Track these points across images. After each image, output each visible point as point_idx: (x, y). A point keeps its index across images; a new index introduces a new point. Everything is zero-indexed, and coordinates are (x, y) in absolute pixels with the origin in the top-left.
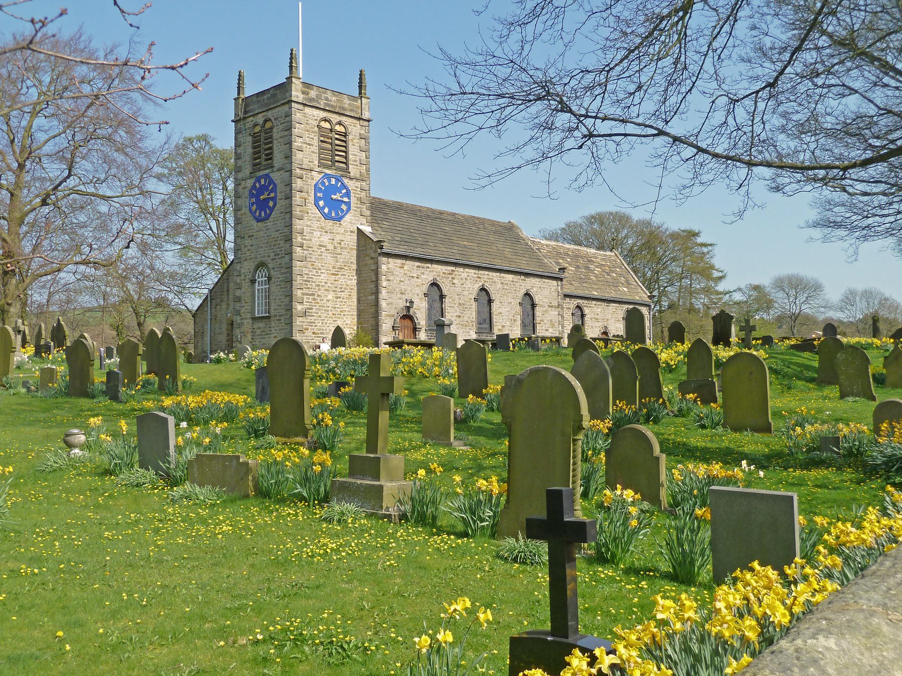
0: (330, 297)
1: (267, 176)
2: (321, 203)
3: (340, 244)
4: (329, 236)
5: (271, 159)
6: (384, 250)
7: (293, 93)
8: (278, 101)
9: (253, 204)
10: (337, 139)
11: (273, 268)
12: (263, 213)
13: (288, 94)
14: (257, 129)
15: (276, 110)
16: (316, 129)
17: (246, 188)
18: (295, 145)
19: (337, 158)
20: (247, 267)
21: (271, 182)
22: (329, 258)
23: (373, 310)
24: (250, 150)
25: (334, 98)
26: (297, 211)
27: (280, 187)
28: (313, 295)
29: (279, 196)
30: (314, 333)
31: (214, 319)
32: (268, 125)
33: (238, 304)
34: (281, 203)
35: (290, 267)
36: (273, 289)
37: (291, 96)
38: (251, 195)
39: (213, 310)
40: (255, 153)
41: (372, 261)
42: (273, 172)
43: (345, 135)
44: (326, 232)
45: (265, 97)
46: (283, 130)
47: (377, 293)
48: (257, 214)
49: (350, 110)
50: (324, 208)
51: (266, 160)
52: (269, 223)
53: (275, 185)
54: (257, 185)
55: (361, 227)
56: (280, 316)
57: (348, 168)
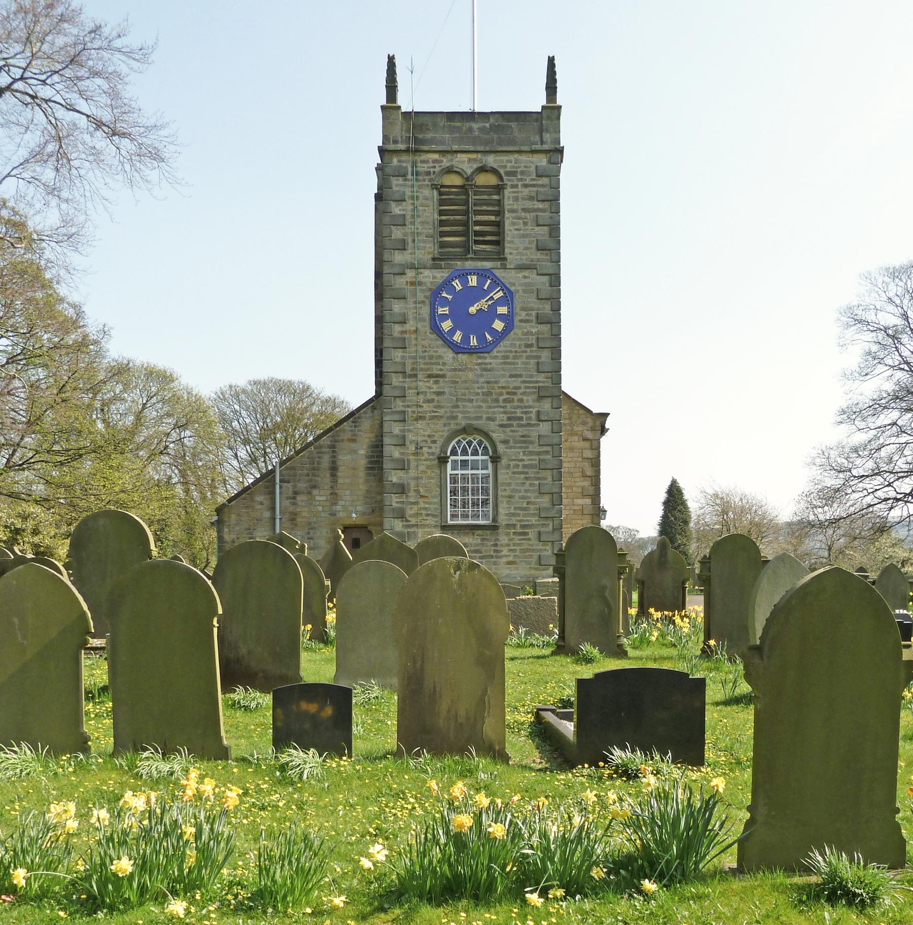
8: (512, 142)
9: (444, 317)
11: (505, 442)
12: (474, 342)
15: (513, 157)
17: (420, 283)
24: (430, 213)
40: (442, 223)
41: (587, 444)
42: (504, 267)
45: (475, 126)
46: (531, 198)
51: (476, 242)
54: (457, 285)
56: (523, 527)
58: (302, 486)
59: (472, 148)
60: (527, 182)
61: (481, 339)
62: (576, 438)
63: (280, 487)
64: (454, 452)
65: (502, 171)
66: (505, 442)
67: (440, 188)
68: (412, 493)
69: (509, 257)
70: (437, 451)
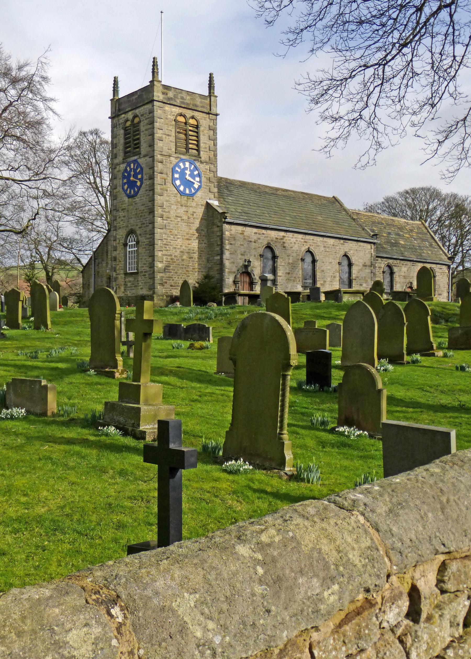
0: (184, 257)
1: (135, 162)
2: (178, 182)
3: (193, 215)
4: (184, 209)
5: (138, 147)
6: (227, 220)
7: (155, 94)
10: (190, 130)
11: (140, 235)
13: (151, 95)
14: (128, 123)
16: (174, 123)
18: (157, 136)
19: (191, 146)
20: (121, 234)
21: (139, 165)
22: (183, 227)
23: (218, 267)
25: (188, 97)
26: (158, 188)
27: (146, 170)
28: (171, 255)
29: (145, 177)
30: (171, 286)
31: (97, 274)
32: (136, 120)
33: (114, 263)
34: (147, 182)
35: (153, 234)
36: (140, 250)
37: (153, 96)
38: (124, 177)
39: (96, 268)
40: (126, 143)
42: (140, 158)
43: (197, 127)
44: (182, 206)
45: (134, 98)
47: (221, 254)
48: (128, 192)
49: (201, 107)
50: (180, 186)
52: (137, 199)
53: (142, 169)
55: (209, 201)
56: (145, 272)
57: (199, 154)
58: (100, 260)
59: (130, 109)
60: (147, 117)
61: (134, 191)
62: (215, 226)
63: (95, 261)
64: (129, 242)
65: (140, 116)
66: (140, 235)
67: (125, 129)
68: (118, 261)
69: (142, 152)
70: (123, 241)
